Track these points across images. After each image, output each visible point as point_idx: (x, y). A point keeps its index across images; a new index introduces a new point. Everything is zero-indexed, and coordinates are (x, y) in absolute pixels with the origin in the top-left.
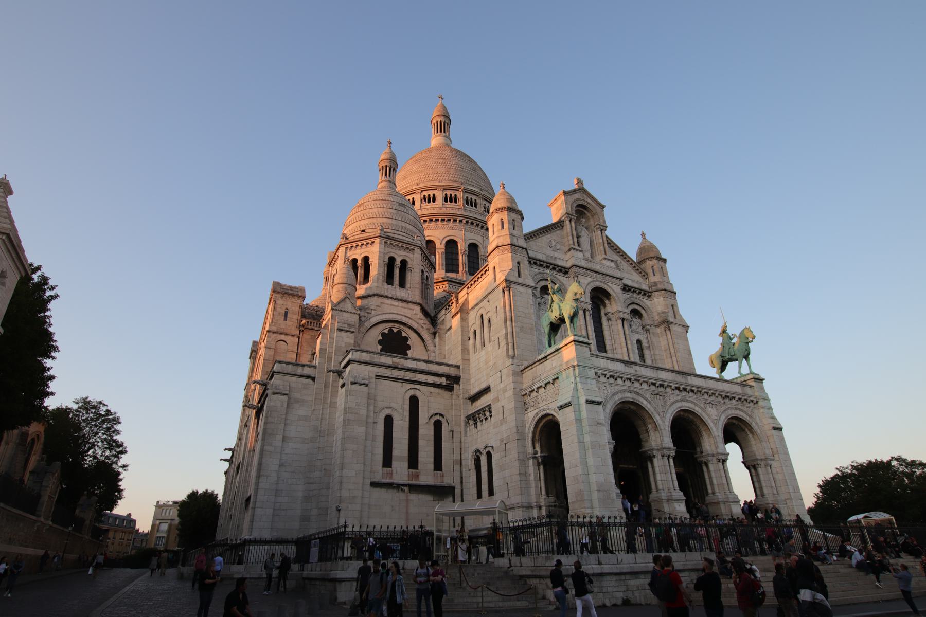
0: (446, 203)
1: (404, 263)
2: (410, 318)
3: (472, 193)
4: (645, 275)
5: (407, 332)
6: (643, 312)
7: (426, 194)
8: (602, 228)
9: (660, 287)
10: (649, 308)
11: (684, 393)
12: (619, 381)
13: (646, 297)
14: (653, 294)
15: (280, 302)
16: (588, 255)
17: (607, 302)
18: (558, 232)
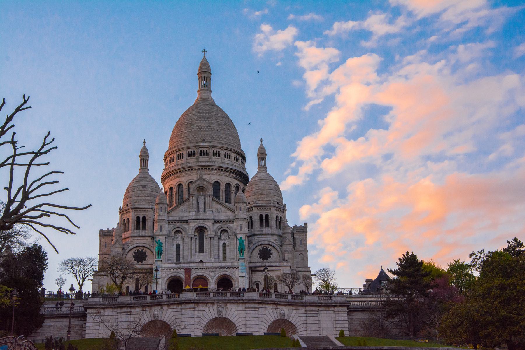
0: (189, 158)
1: (144, 218)
2: (146, 244)
3: (204, 147)
4: (233, 211)
5: (145, 250)
6: (228, 230)
7: (178, 153)
8: (209, 195)
9: (236, 217)
10: (231, 227)
11: (200, 270)
12: (172, 270)
13: (230, 223)
14: (235, 220)
15: (103, 240)
16: (201, 210)
17: (206, 231)
18: (188, 203)
